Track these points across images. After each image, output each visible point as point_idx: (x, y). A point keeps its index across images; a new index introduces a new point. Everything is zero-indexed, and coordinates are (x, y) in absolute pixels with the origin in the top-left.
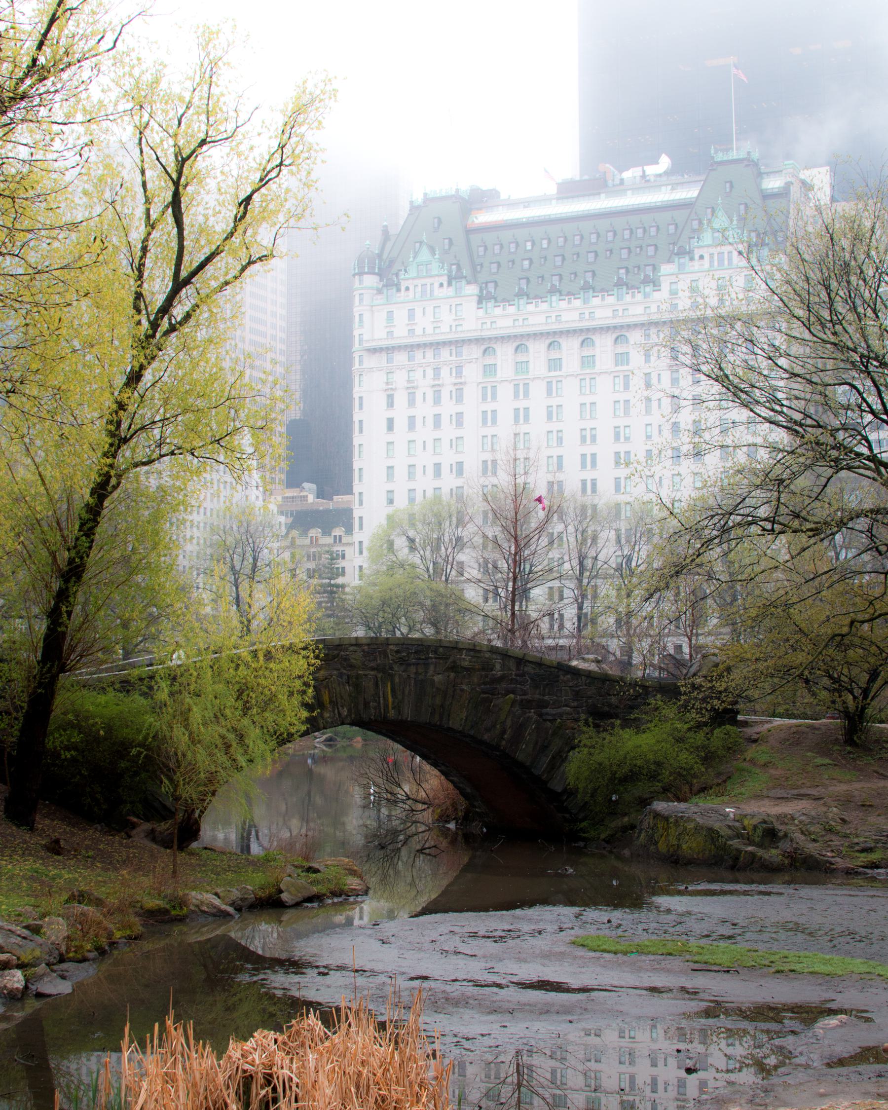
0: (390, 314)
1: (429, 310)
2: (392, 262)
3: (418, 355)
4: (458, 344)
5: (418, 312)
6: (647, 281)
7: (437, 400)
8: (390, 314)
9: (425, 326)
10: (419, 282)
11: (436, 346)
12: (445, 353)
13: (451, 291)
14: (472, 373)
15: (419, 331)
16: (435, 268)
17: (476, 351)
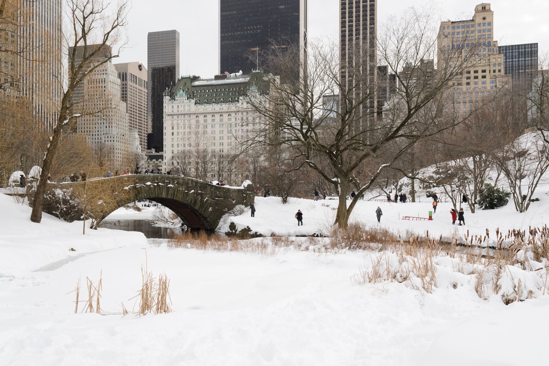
0: (173, 106)
1: (183, 106)
2: (173, 94)
3: (180, 117)
4: (189, 114)
5: (180, 106)
6: (236, 101)
7: (184, 128)
8: (173, 106)
9: (181, 109)
10: (180, 98)
11: (184, 114)
12: (186, 116)
13: (188, 101)
14: (193, 121)
15: (180, 111)
16: (184, 94)
17: (194, 116)
